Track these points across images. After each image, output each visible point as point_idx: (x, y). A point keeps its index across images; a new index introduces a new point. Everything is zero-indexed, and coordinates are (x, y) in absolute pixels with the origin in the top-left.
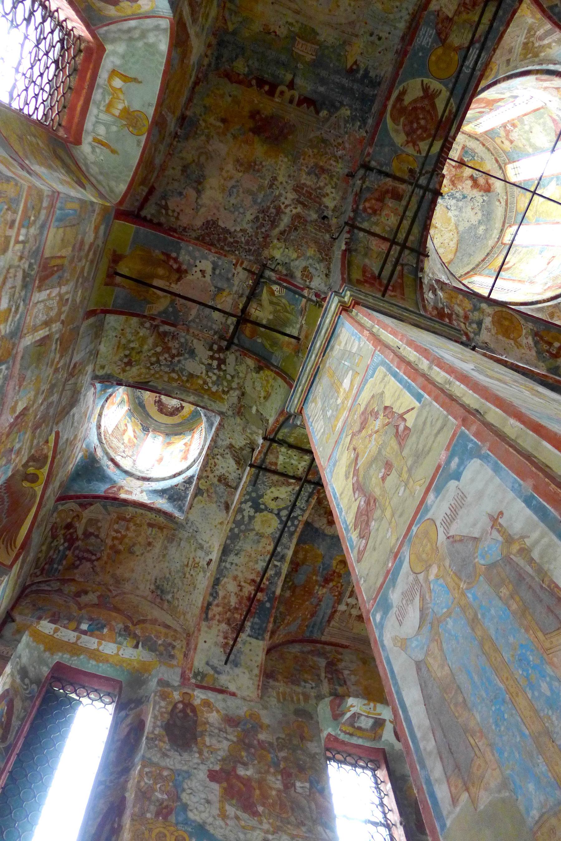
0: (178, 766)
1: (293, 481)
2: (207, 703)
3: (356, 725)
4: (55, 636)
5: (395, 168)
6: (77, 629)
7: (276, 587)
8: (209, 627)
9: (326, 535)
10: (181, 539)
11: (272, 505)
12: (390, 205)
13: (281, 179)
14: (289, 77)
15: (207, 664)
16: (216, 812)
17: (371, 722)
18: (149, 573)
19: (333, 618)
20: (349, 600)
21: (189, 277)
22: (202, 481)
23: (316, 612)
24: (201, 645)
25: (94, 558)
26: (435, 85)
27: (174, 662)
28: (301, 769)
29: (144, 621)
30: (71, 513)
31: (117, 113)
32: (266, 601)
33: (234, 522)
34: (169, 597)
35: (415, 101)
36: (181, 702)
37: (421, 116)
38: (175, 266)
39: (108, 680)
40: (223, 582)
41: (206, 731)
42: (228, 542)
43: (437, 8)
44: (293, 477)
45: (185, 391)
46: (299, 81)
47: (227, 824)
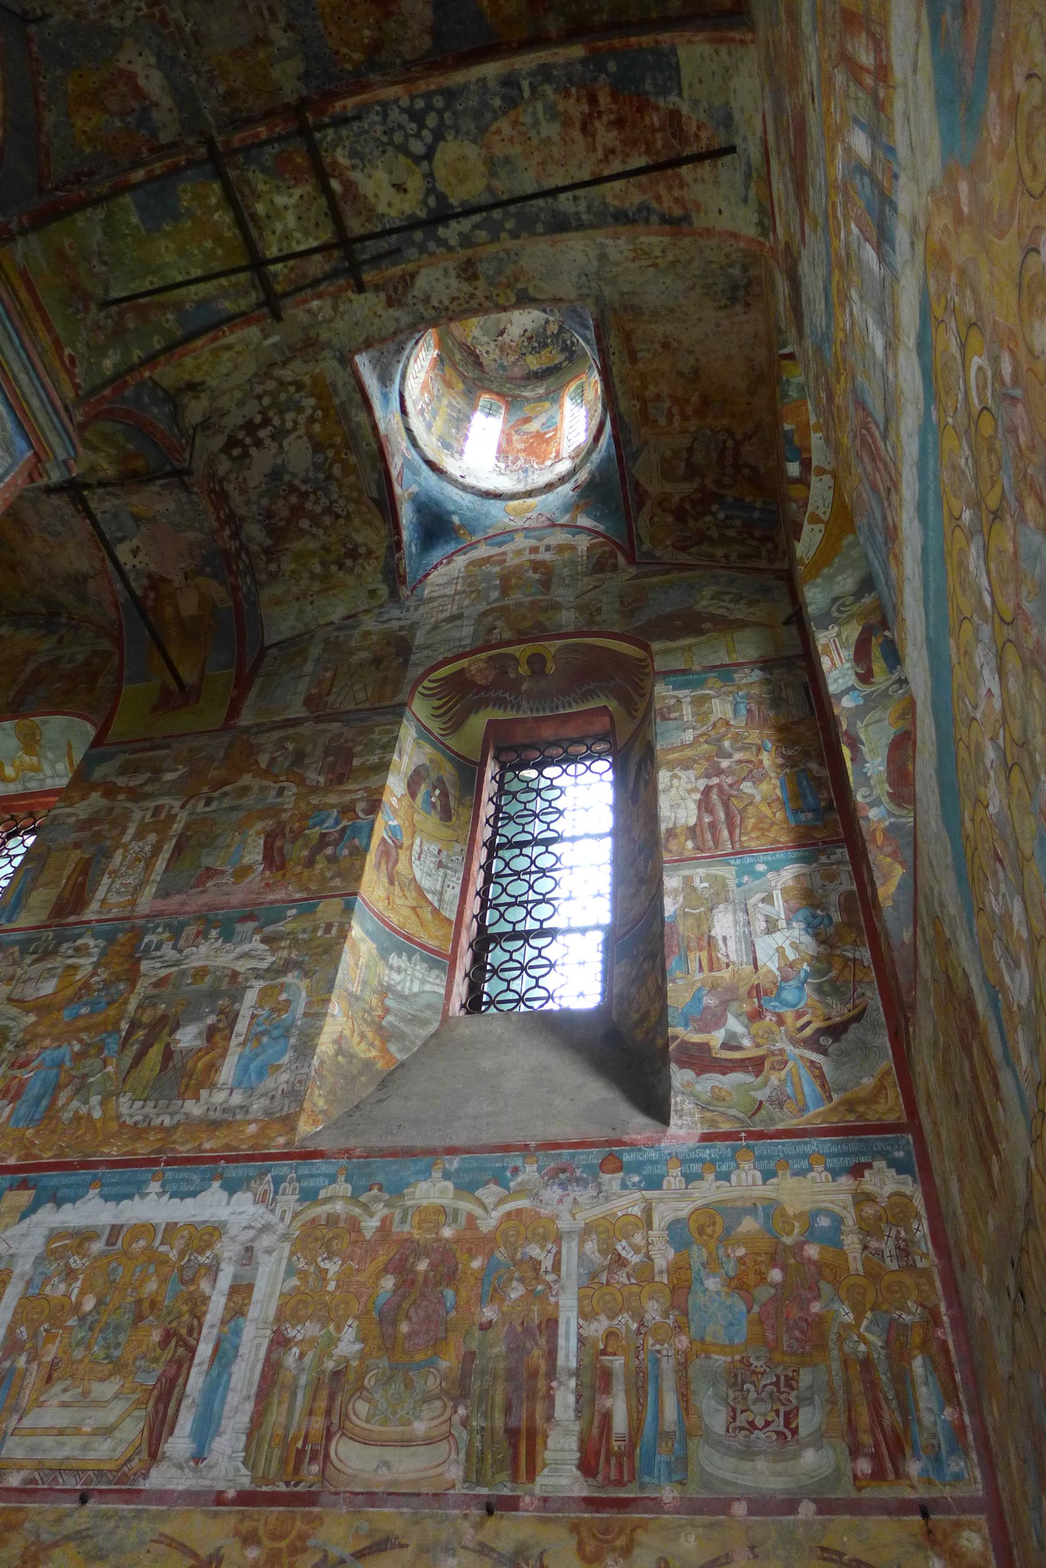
1: (335, 184)
4: (825, 518)
6: (804, 481)
10: (622, 294)
11: (415, 183)
18: (718, 325)
21: (152, 567)
22: (502, 301)
25: (730, 443)
30: (656, 519)
31: (35, 759)
32: (608, 74)
33: (495, 239)
34: (736, 271)
38: (152, 595)
40: (617, 203)
42: (540, 228)
44: (326, 190)
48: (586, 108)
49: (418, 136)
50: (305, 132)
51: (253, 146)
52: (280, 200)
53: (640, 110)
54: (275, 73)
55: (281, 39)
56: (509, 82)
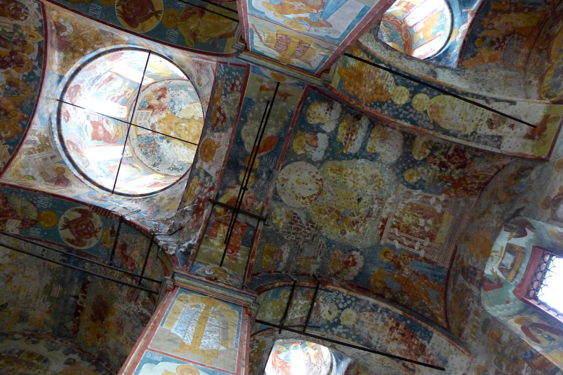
1: (315, 304)
3: (509, 267)
5: (110, 246)
7: (397, 313)
9: (364, 266)
11: (335, 314)
12: (129, 252)
13: (125, 309)
14: (72, 299)
17: (508, 255)
19: (430, 260)
20: (416, 248)
23: (423, 275)
26: (62, 222)
32: (406, 323)
35: (72, 232)
37: (80, 228)
43: (18, 230)
44: (312, 305)
45: (260, 361)
46: (74, 293)
48: (394, 325)
49: (343, 303)
50: (317, 289)
51: (303, 286)
52: (300, 302)
53: (412, 337)
54: (312, 266)
55: (319, 259)
56: (375, 306)
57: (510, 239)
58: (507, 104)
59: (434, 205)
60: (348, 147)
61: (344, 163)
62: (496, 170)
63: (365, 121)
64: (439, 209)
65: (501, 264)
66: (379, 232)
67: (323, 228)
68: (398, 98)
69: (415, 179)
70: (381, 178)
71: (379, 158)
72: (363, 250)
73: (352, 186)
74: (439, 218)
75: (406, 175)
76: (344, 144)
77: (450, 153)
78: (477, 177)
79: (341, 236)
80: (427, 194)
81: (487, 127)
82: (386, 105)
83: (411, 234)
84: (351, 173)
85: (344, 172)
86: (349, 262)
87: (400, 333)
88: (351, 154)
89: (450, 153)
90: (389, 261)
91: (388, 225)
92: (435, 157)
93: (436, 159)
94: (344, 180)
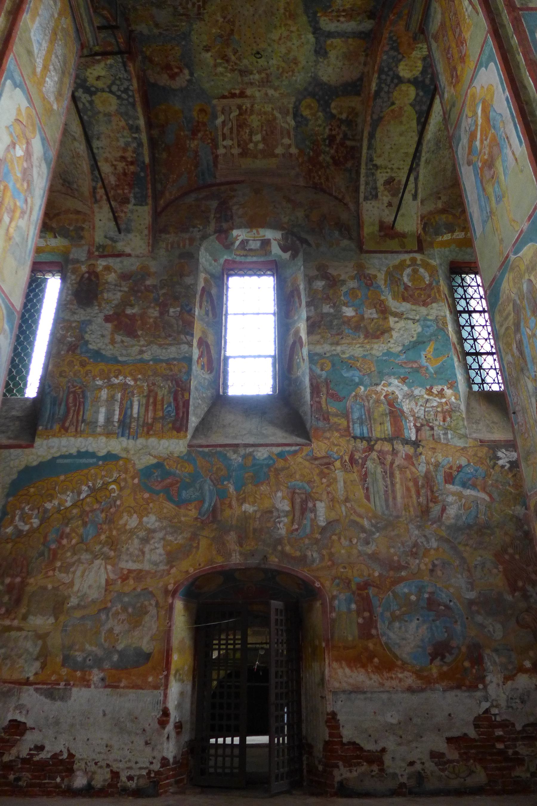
0: (83, 318)
2: (107, 268)
3: (247, 248)
8: (101, 208)
11: (100, 84)
15: (106, 237)
16: (107, 341)
17: (258, 244)
20: (225, 143)
24: (98, 224)
27: (83, 242)
28: (176, 298)
29: (58, 214)
36: (87, 272)
39: (51, 263)
41: (105, 288)
47: (115, 347)
48: (129, 159)
49: (119, 90)
50: (120, 52)
53: (129, 185)
56: (137, 129)
57: (275, 240)
58: (413, 192)
59: (282, 144)
60: (326, 16)
61: (303, 19)
62: (340, 197)
63: (368, 25)
64: (279, 150)
65: (247, 241)
66: (226, 94)
67: (203, 22)
68: (406, 65)
69: (306, 113)
70: (296, 70)
71: (321, 60)
72: (194, 81)
73: (274, 38)
74: (269, 153)
75: (309, 100)
76: (330, 10)
77: (349, 143)
78: (327, 179)
79: (202, 47)
80: (292, 133)
81: (385, 179)
82: (396, 53)
83: (238, 131)
84: (292, 32)
85: (290, 22)
86: (171, 69)
87: (124, 169)
88: (317, 22)
89: (349, 143)
90: (196, 119)
91: (239, 101)
92: (339, 127)
93: (337, 129)
94: (278, 25)
